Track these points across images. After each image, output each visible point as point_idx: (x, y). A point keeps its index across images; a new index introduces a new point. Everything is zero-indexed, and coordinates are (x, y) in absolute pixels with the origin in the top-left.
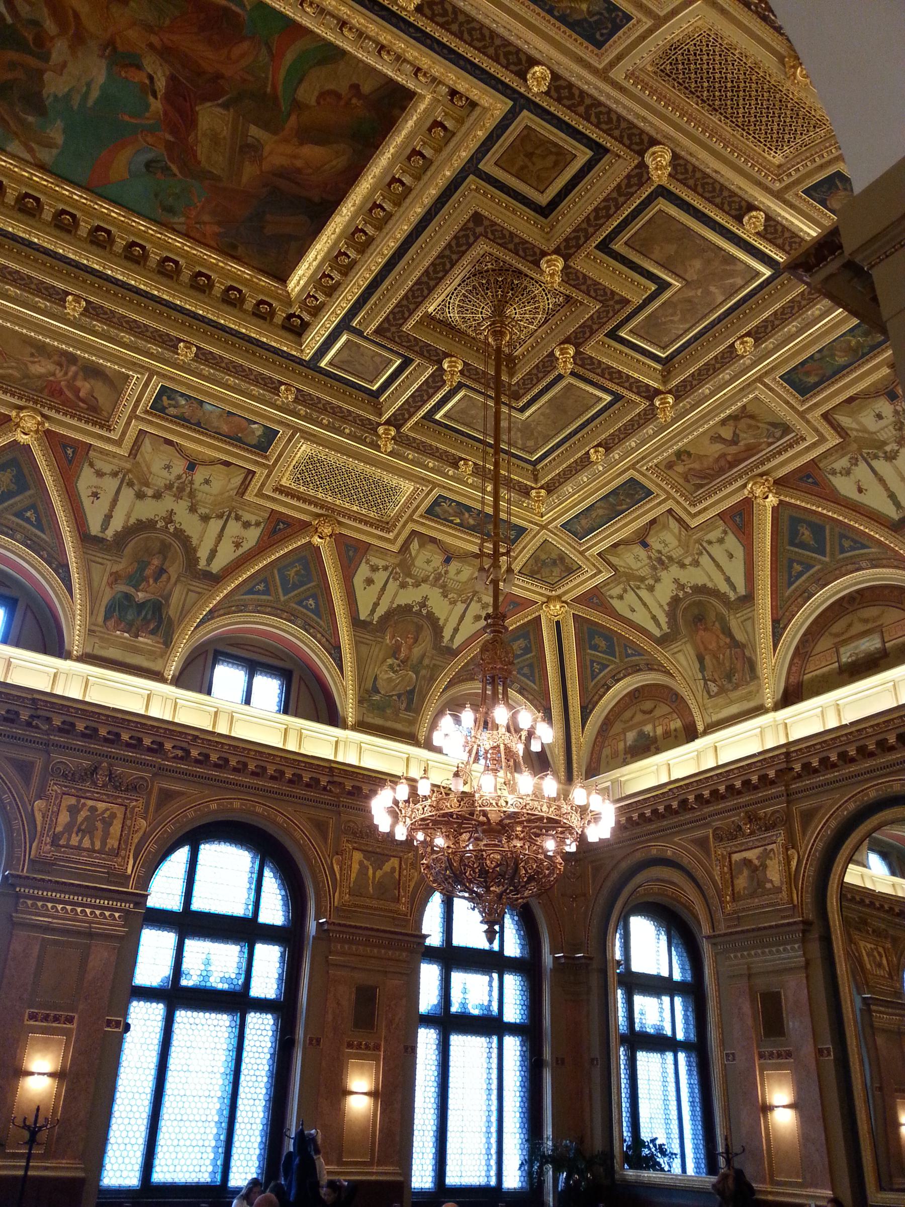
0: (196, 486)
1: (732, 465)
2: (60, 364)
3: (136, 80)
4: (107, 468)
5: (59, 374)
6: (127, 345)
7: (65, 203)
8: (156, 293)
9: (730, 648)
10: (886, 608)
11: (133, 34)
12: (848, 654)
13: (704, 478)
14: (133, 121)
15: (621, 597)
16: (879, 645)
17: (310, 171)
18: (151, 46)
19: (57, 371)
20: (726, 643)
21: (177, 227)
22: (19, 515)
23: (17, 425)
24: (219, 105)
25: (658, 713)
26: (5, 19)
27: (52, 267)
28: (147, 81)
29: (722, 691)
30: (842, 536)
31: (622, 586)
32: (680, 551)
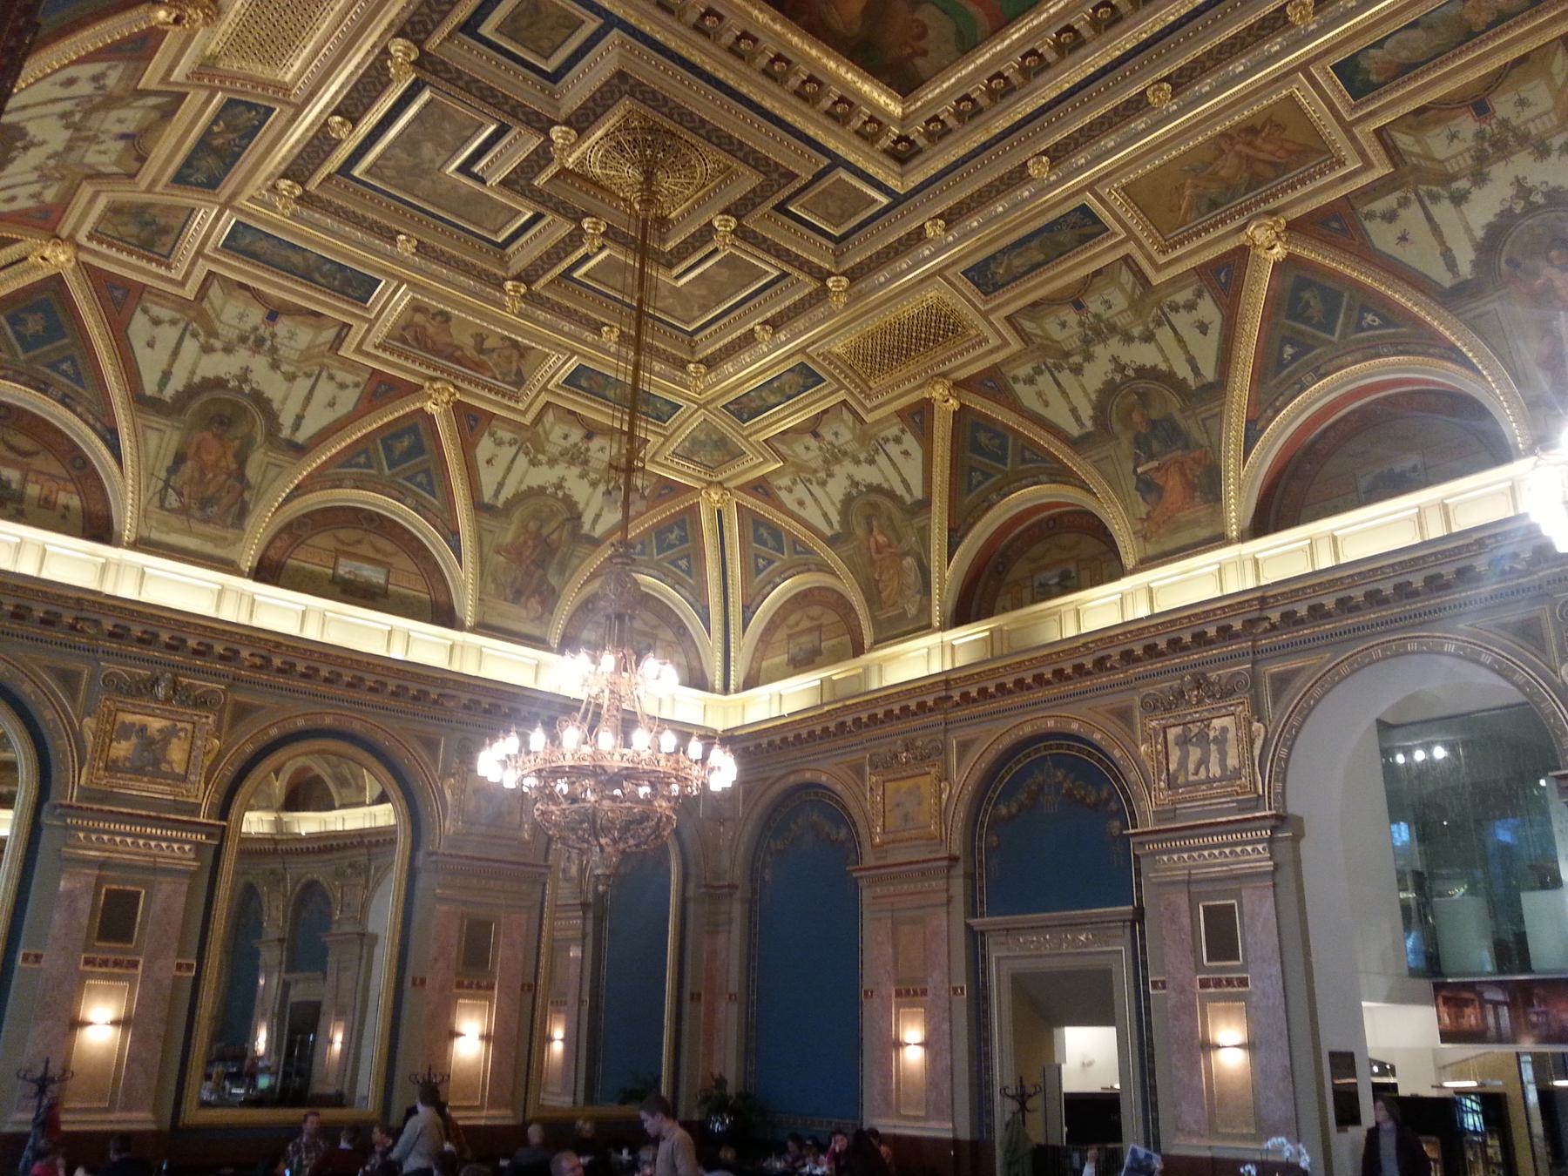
1: (450, 358)
9: (230, 475)
10: (401, 553)
12: (347, 569)
13: (417, 339)
15: (157, 322)
16: (382, 582)
20: (228, 468)
25: (38, 463)
29: (184, 511)
30: (427, 472)
31: (178, 316)
32: (295, 356)
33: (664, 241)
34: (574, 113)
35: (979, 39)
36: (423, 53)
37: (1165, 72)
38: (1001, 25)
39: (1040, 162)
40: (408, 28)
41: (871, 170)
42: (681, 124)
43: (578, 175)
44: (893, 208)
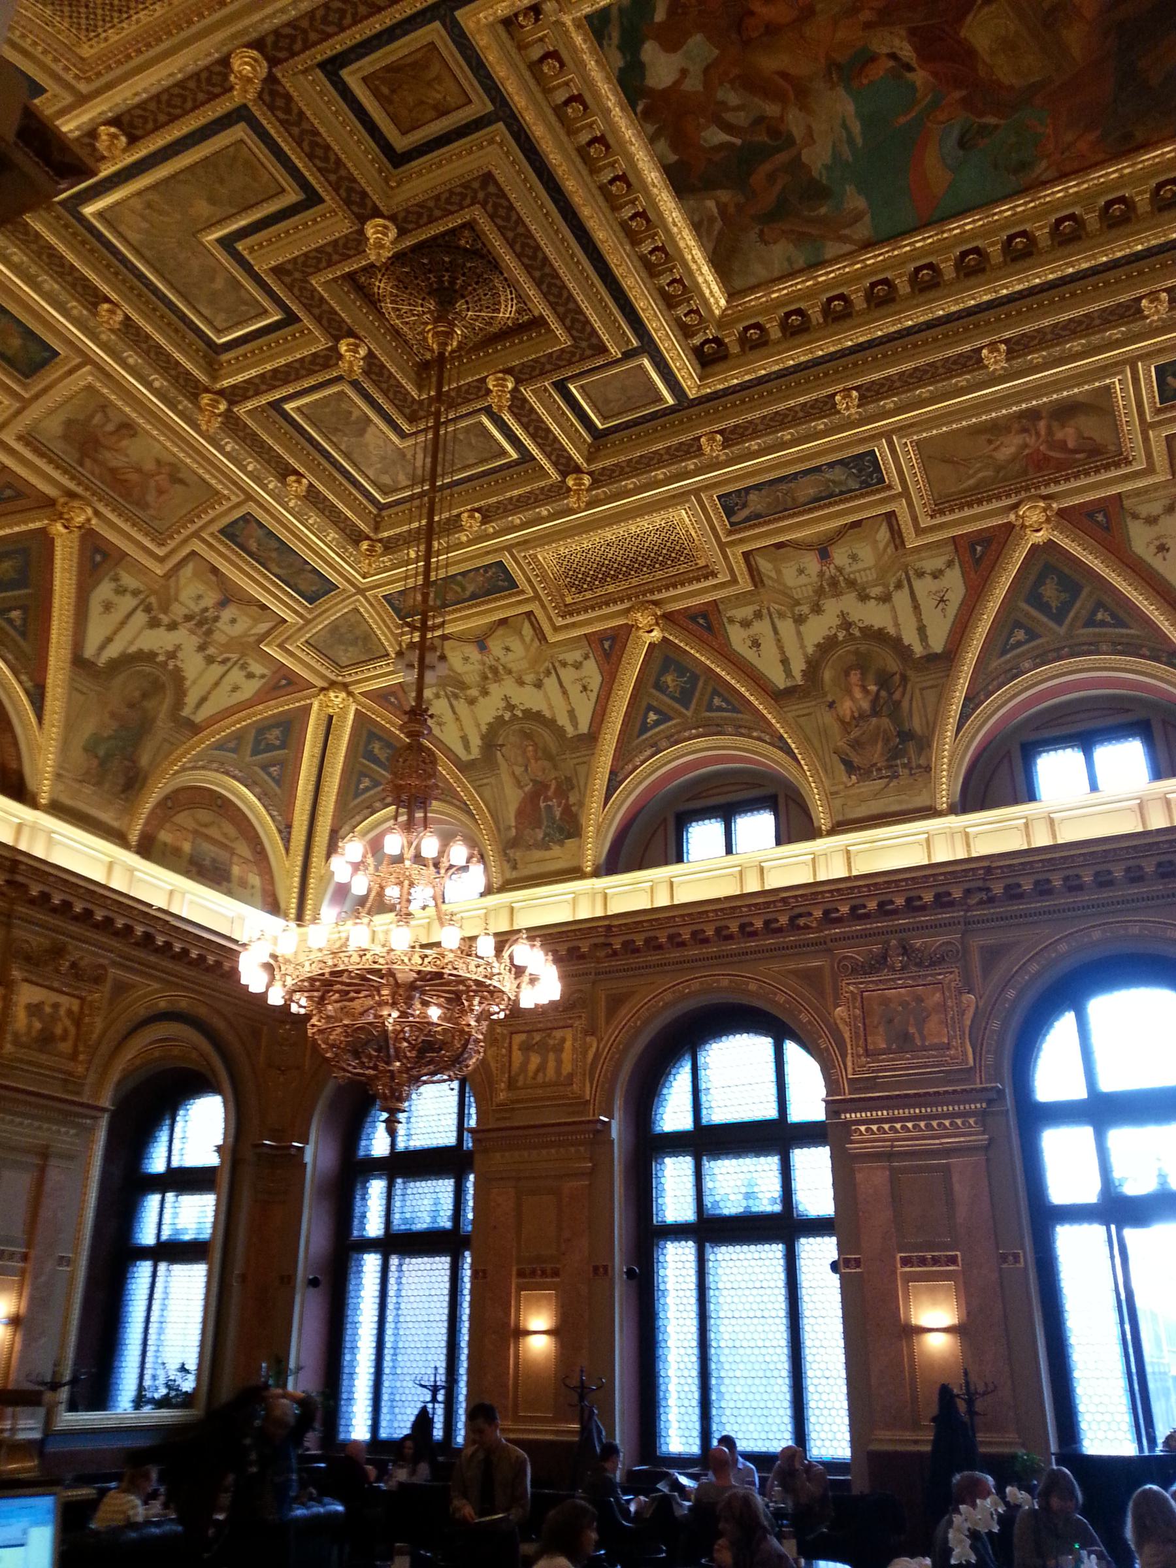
2: (1025, 430)
3: (881, 73)
4: (1156, 508)
6: (1084, 352)
7: (914, 260)
8: (1071, 270)
11: (840, 35)
14: (908, 117)
18: (868, 26)
21: (1044, 178)
22: (1090, 622)
23: (1023, 527)
24: (981, 7)
26: (733, 144)
27: (946, 336)
28: (891, 63)
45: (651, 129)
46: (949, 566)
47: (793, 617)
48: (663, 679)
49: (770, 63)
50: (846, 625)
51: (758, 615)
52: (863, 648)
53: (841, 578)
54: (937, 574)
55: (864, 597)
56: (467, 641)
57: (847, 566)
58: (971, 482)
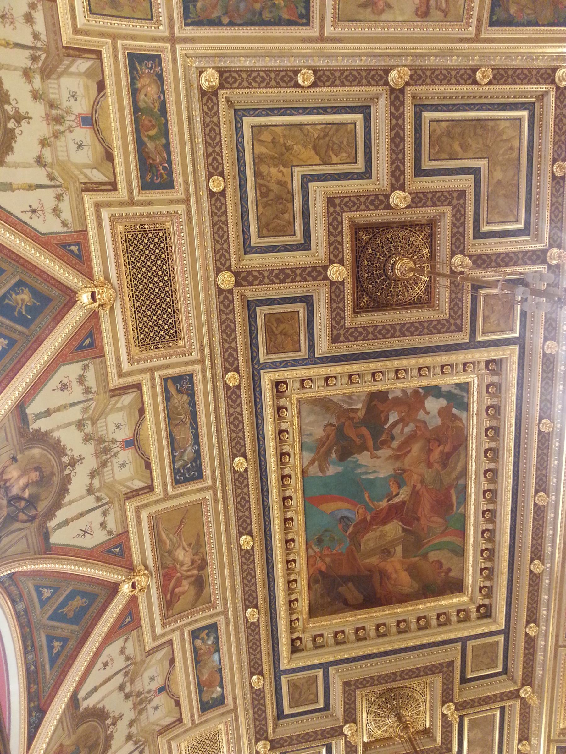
0: (149, 706)
2: (193, 562)
4: (130, 651)
5: (185, 568)
17: (393, 583)
18: (414, 486)
19: (186, 566)
21: (310, 550)
22: (50, 639)
26: (386, 424)
28: (394, 494)
33: (435, 740)
34: (345, 716)
35: (462, 546)
36: (271, 741)
37: (533, 491)
38: (463, 534)
39: (535, 564)
40: (258, 736)
41: (479, 631)
42: (387, 683)
43: (374, 741)
44: (509, 637)
45: (409, 392)
46: (108, 532)
47: (83, 420)
48: (26, 291)
49: (416, 448)
50: (73, 463)
51: (87, 391)
52: (55, 479)
53: (108, 456)
54: (103, 525)
55: (92, 475)
56: (94, 109)
57: (117, 460)
58: (164, 536)
